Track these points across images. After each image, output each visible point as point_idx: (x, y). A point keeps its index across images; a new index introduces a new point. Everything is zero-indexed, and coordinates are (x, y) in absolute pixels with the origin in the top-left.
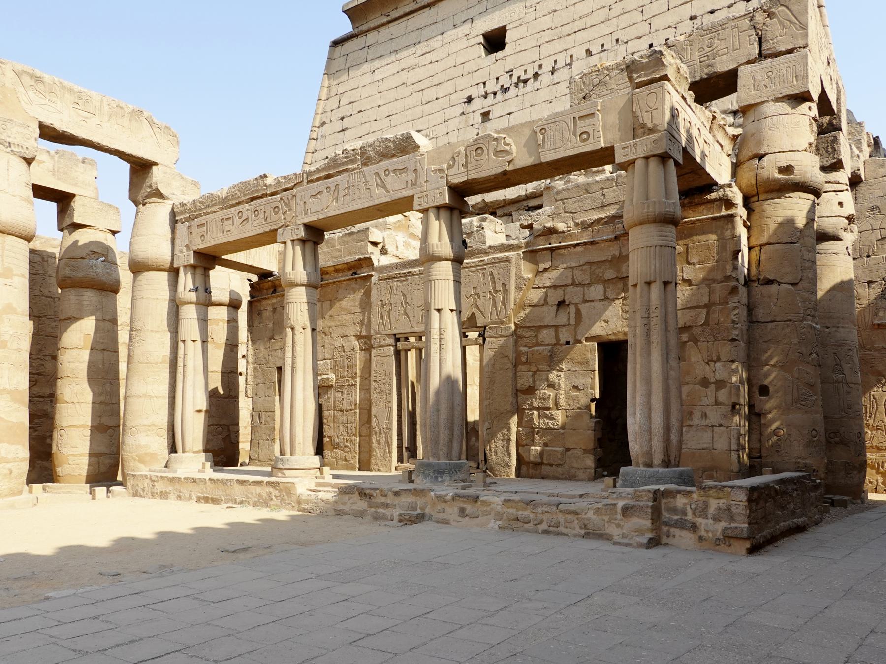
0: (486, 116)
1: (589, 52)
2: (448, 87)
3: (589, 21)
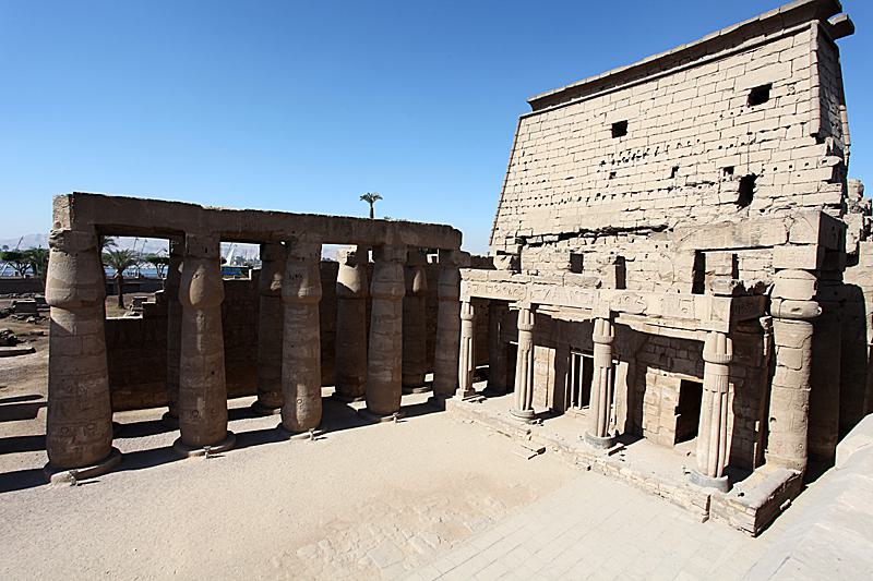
2: (590, 154)
3: (681, 126)
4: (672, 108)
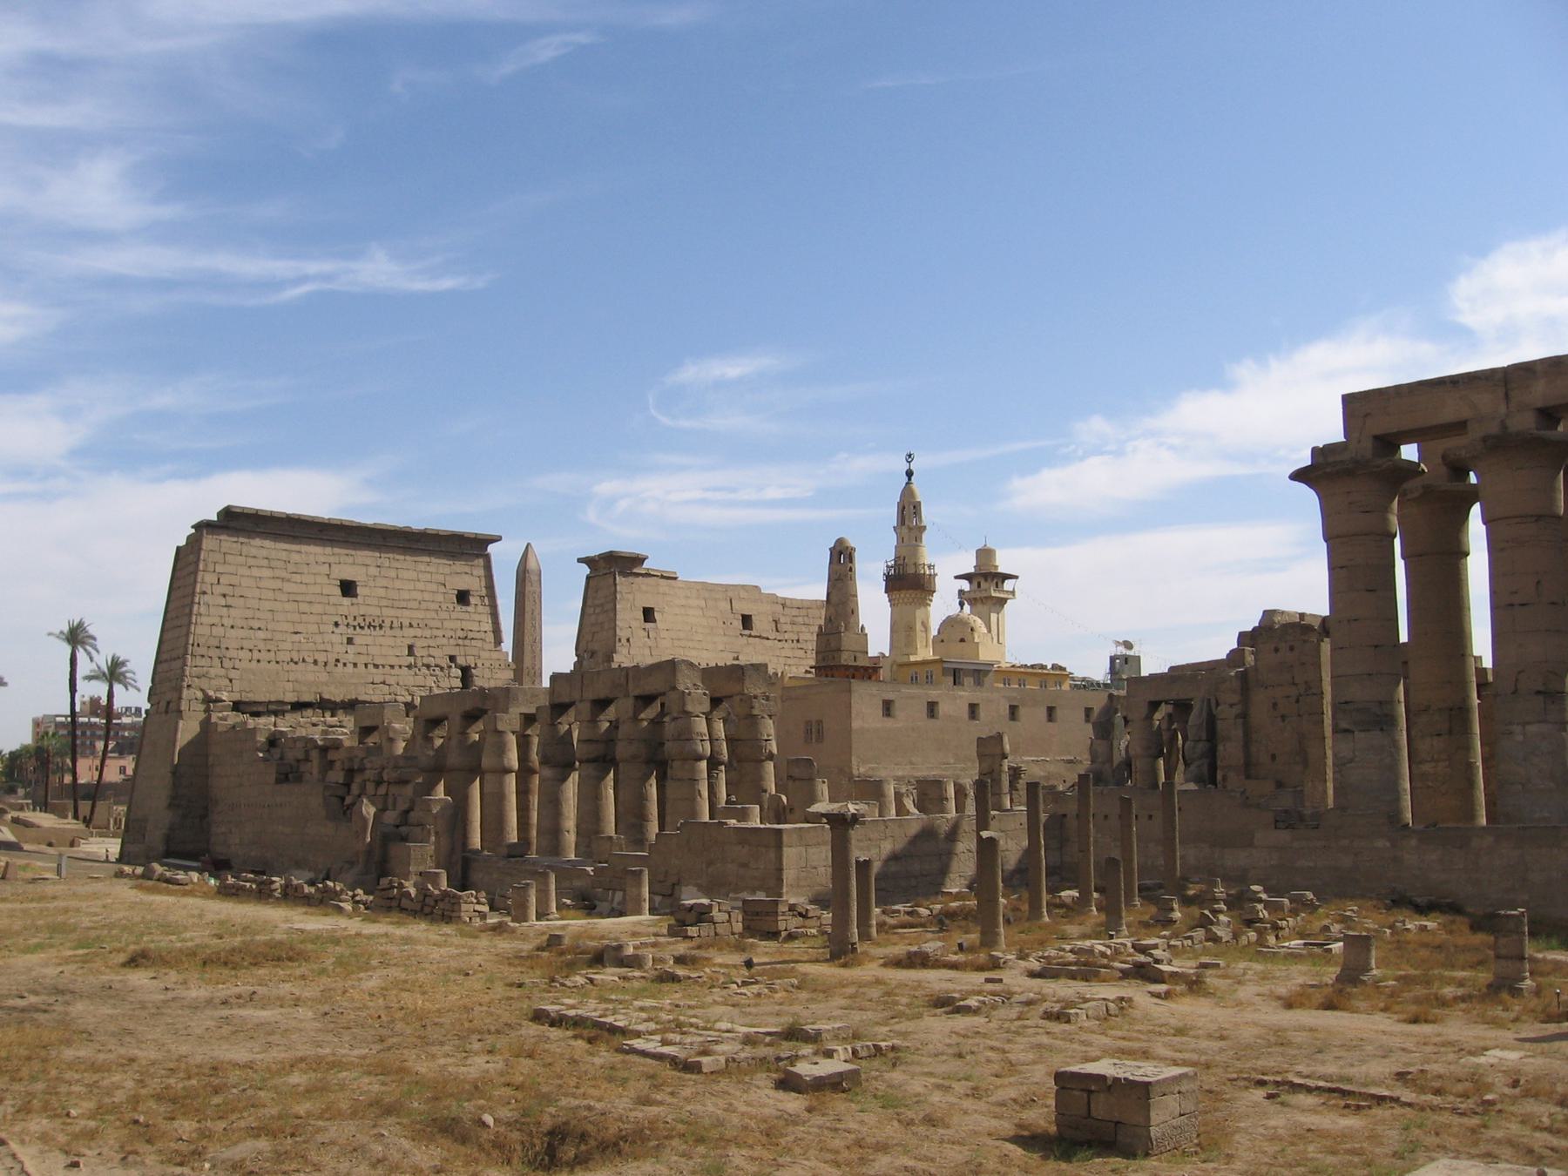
0: (350, 641)
4: (398, 584)
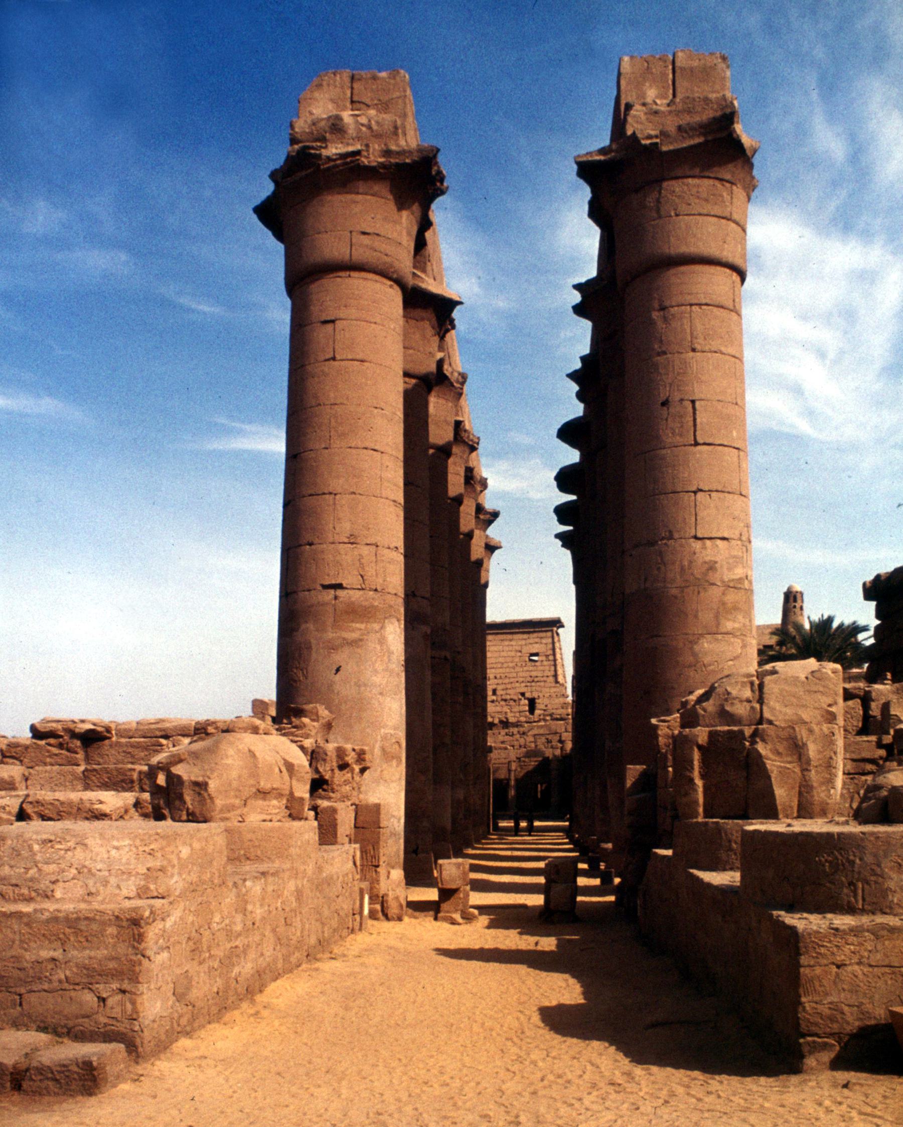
1: (496, 678)
